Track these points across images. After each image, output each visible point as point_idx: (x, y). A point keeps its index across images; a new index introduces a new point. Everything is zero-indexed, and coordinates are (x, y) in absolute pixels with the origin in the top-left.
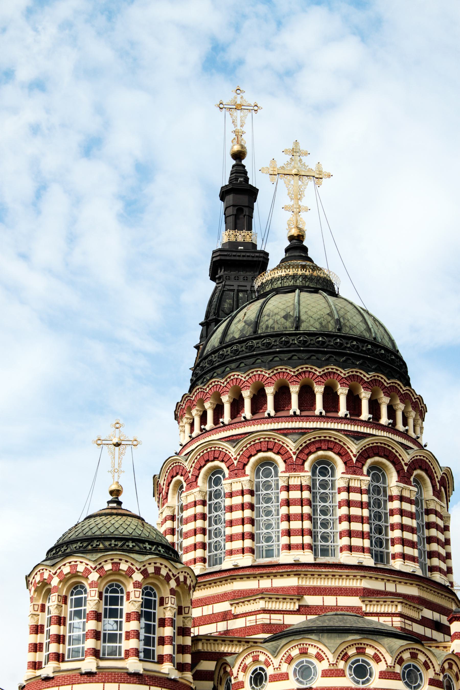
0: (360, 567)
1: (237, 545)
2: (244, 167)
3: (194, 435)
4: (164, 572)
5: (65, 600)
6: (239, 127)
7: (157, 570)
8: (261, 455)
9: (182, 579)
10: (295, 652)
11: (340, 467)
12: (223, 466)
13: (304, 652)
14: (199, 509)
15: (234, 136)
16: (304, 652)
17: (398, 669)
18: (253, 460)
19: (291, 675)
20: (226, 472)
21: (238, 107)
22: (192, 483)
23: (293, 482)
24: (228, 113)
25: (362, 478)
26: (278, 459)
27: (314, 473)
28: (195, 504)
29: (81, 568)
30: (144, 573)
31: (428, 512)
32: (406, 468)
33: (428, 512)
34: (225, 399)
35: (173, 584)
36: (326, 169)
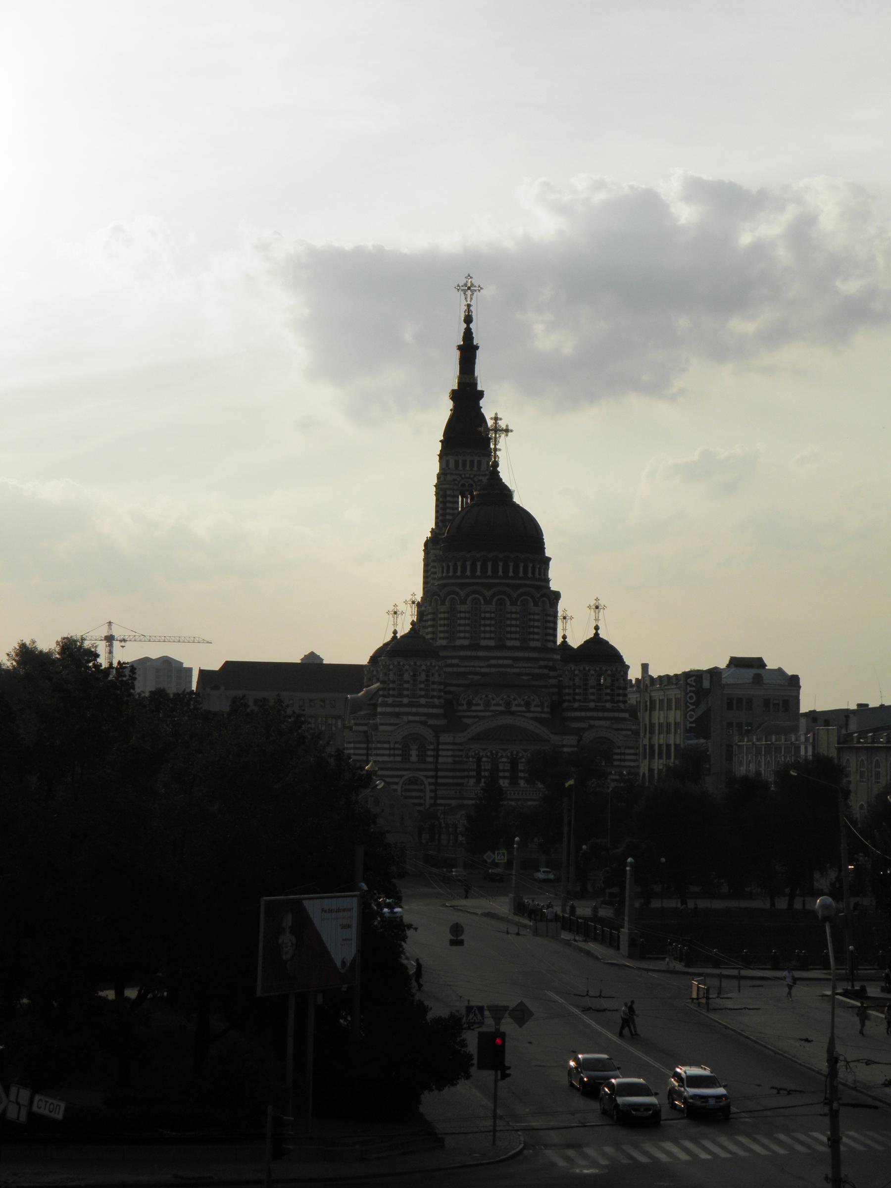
0: (513, 648)
1: (462, 635)
3: (444, 575)
4: (433, 664)
5: (395, 674)
6: (469, 303)
7: (431, 664)
8: (474, 596)
9: (440, 665)
10: (483, 696)
11: (508, 602)
12: (457, 598)
13: (487, 696)
14: (446, 615)
15: (466, 308)
16: (487, 696)
17: (522, 703)
18: (470, 598)
19: (482, 705)
20: (458, 602)
21: (469, 288)
22: (443, 603)
23: (488, 609)
24: (462, 293)
25: (517, 607)
26: (481, 598)
27: (496, 605)
28: (444, 612)
29: (402, 663)
30: (426, 665)
31: (547, 615)
32: (537, 600)
33: (547, 615)
34: (459, 564)
35: (437, 668)
36: (510, 428)
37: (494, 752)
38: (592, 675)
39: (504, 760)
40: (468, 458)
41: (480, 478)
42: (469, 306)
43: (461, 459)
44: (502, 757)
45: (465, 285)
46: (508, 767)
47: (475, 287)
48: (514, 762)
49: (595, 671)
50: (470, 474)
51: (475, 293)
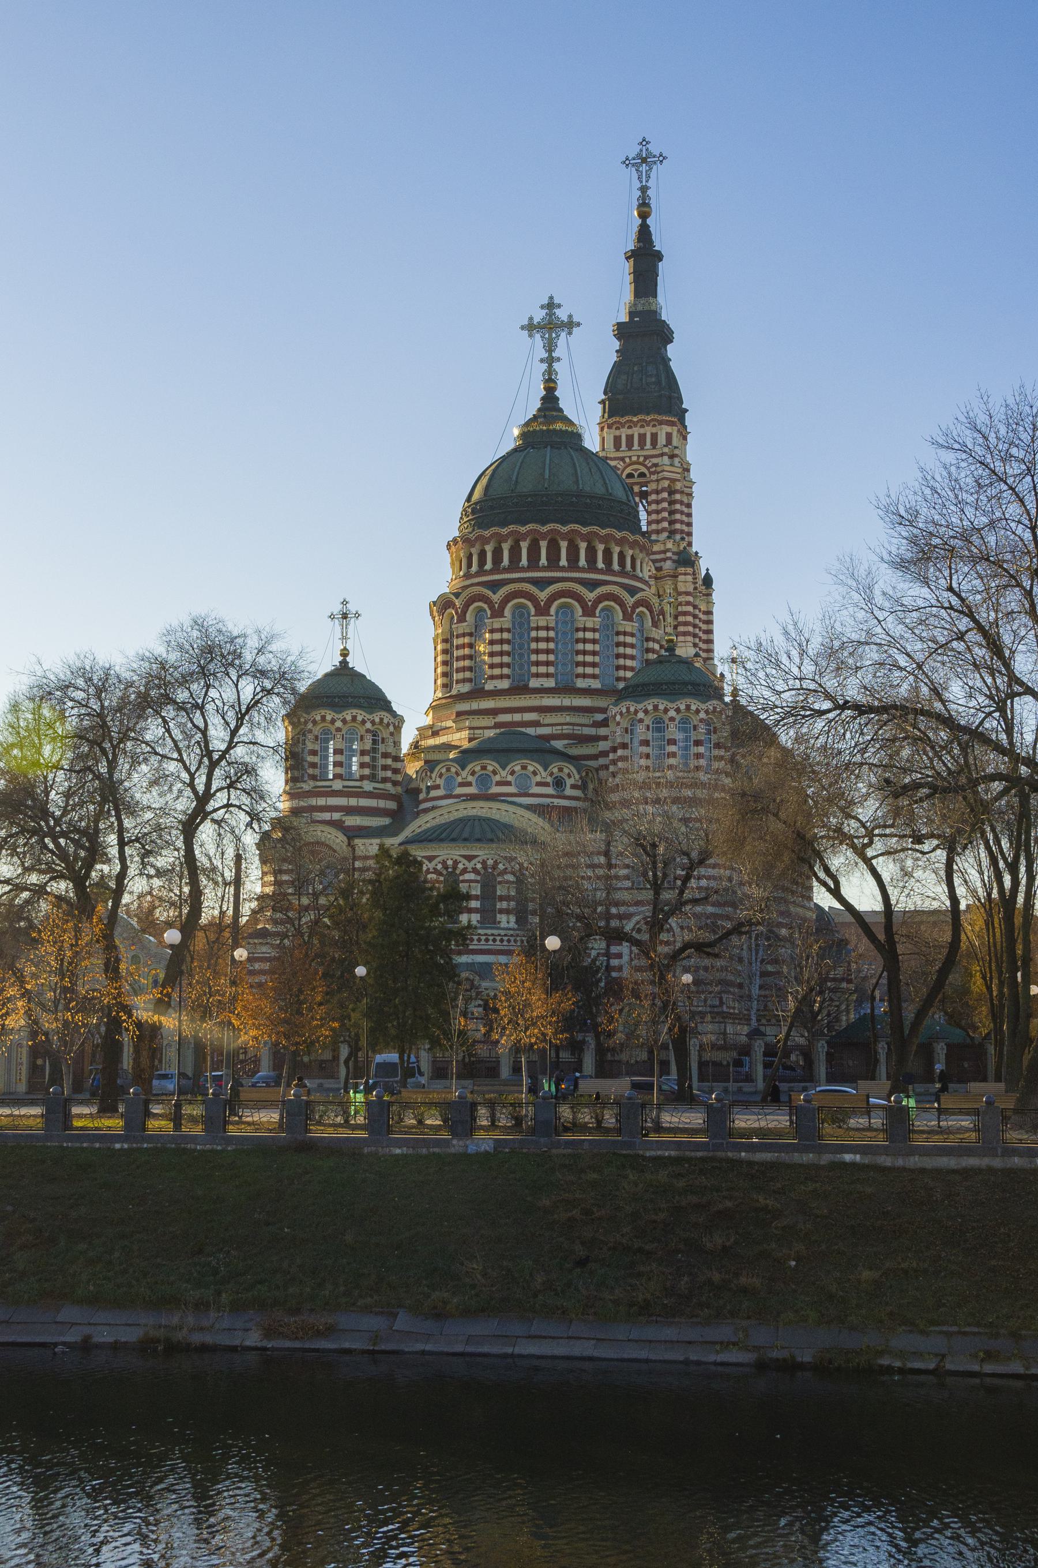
2: (648, 226)
15: (639, 193)
21: (644, 160)
24: (634, 169)
37: (450, 863)
38: (672, 719)
39: (467, 876)
40: (636, 432)
41: (655, 461)
42: (644, 189)
43: (624, 432)
44: (464, 871)
45: (639, 156)
46: (476, 890)
47: (654, 157)
48: (488, 882)
49: (678, 710)
50: (639, 456)
51: (655, 167)
